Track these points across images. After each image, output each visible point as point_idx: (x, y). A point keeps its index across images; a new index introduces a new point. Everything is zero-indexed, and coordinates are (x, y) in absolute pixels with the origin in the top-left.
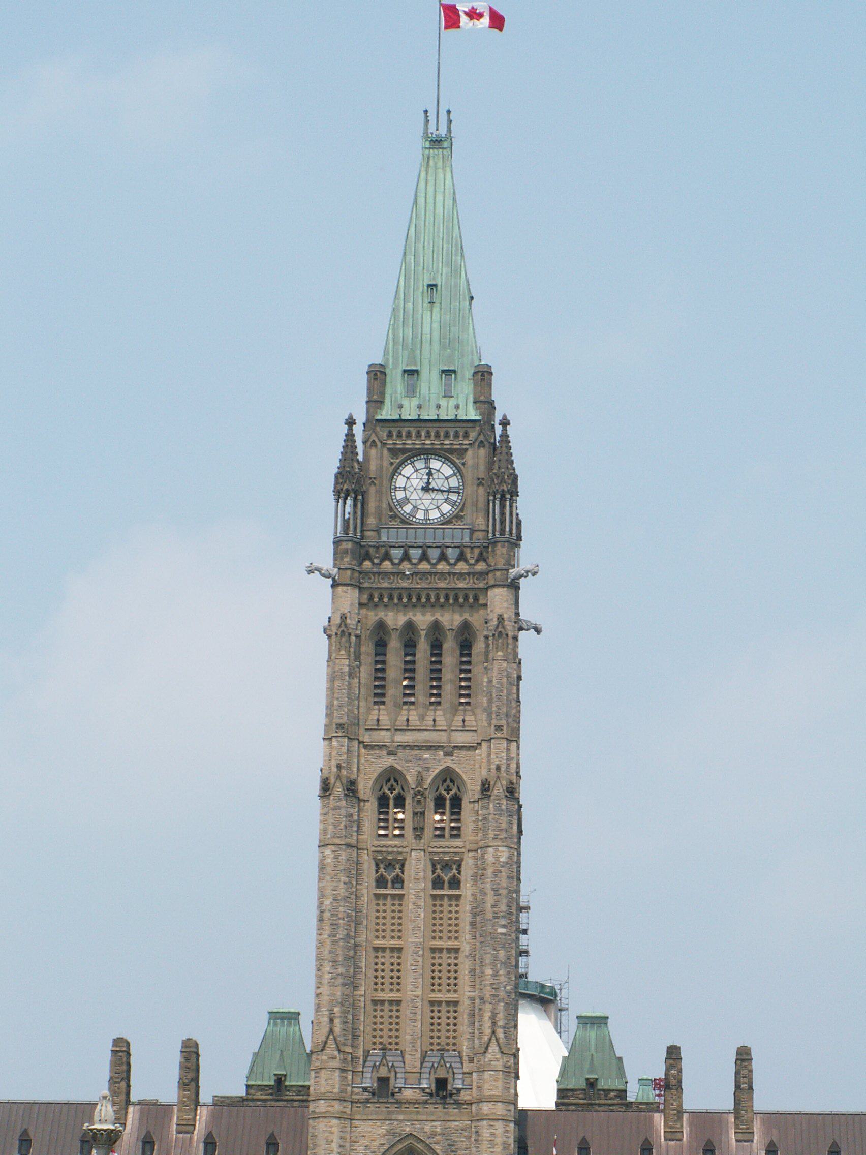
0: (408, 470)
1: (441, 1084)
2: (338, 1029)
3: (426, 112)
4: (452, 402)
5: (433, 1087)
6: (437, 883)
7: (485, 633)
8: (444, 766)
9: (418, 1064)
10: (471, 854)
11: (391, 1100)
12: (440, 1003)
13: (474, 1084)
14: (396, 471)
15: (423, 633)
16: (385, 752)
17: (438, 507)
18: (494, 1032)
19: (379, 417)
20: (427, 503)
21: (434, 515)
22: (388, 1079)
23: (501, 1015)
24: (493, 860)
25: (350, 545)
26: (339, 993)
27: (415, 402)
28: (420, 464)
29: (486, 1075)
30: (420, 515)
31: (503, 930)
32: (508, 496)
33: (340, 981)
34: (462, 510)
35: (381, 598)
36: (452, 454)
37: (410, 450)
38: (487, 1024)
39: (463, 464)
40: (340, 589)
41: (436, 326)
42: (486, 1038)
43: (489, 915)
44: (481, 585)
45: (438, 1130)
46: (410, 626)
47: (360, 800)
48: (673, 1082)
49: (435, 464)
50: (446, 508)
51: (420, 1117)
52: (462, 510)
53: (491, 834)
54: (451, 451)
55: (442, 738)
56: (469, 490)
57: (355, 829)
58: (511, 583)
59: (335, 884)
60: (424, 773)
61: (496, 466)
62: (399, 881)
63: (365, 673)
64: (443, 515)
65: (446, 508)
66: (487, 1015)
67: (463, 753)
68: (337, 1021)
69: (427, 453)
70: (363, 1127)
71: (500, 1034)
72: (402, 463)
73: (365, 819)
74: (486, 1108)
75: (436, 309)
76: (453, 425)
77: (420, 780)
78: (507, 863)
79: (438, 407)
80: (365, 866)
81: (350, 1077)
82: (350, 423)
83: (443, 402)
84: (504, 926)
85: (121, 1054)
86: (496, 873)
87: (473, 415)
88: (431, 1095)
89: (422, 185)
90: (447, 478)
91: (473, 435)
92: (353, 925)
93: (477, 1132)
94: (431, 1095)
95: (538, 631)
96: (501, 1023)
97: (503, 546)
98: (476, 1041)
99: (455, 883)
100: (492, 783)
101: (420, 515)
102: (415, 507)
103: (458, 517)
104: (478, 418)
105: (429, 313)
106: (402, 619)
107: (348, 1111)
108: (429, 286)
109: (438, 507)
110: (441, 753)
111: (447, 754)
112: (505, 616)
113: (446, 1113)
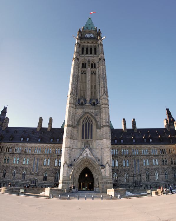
1: (94, 103)
5: (92, 103)
6: (92, 74)
9: (89, 99)
12: (93, 91)
18: (104, 92)
22: (83, 102)
29: (103, 100)
38: (103, 91)
42: (103, 93)
43: (102, 74)
45: (94, 111)
53: (101, 64)
55: (92, 56)
62: (85, 74)
63: (81, 49)
66: (103, 90)
68: (73, 90)
70: (77, 110)
71: (106, 93)
74: (103, 106)
77: (89, 60)
80: (80, 70)
81: (75, 101)
85: (41, 120)
86: (103, 69)
92: (77, 77)
93: (102, 111)
94: (92, 105)
98: (101, 95)
99: (95, 74)
107: (75, 107)
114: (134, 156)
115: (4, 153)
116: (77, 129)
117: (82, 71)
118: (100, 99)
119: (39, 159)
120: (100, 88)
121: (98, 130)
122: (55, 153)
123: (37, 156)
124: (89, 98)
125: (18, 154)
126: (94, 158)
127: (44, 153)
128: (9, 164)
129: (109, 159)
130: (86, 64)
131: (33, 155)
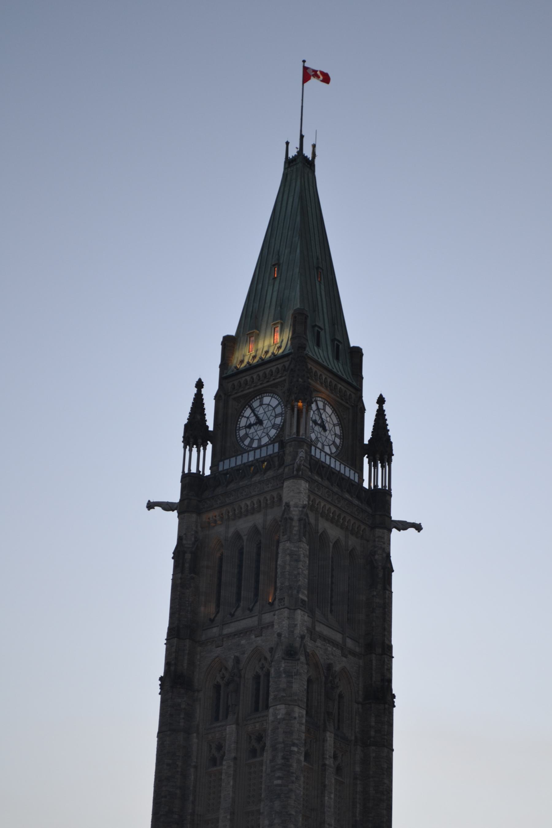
3: (287, 143)
15: (245, 538)
30: (255, 445)
31: (279, 782)
41: (275, 294)
46: (238, 536)
49: (266, 400)
72: (243, 408)
78: (284, 719)
82: (200, 385)
84: (279, 778)
89: (281, 196)
90: (274, 409)
95: (418, 527)
105: (272, 286)
106: (232, 530)
110: (253, 637)
112: (292, 503)
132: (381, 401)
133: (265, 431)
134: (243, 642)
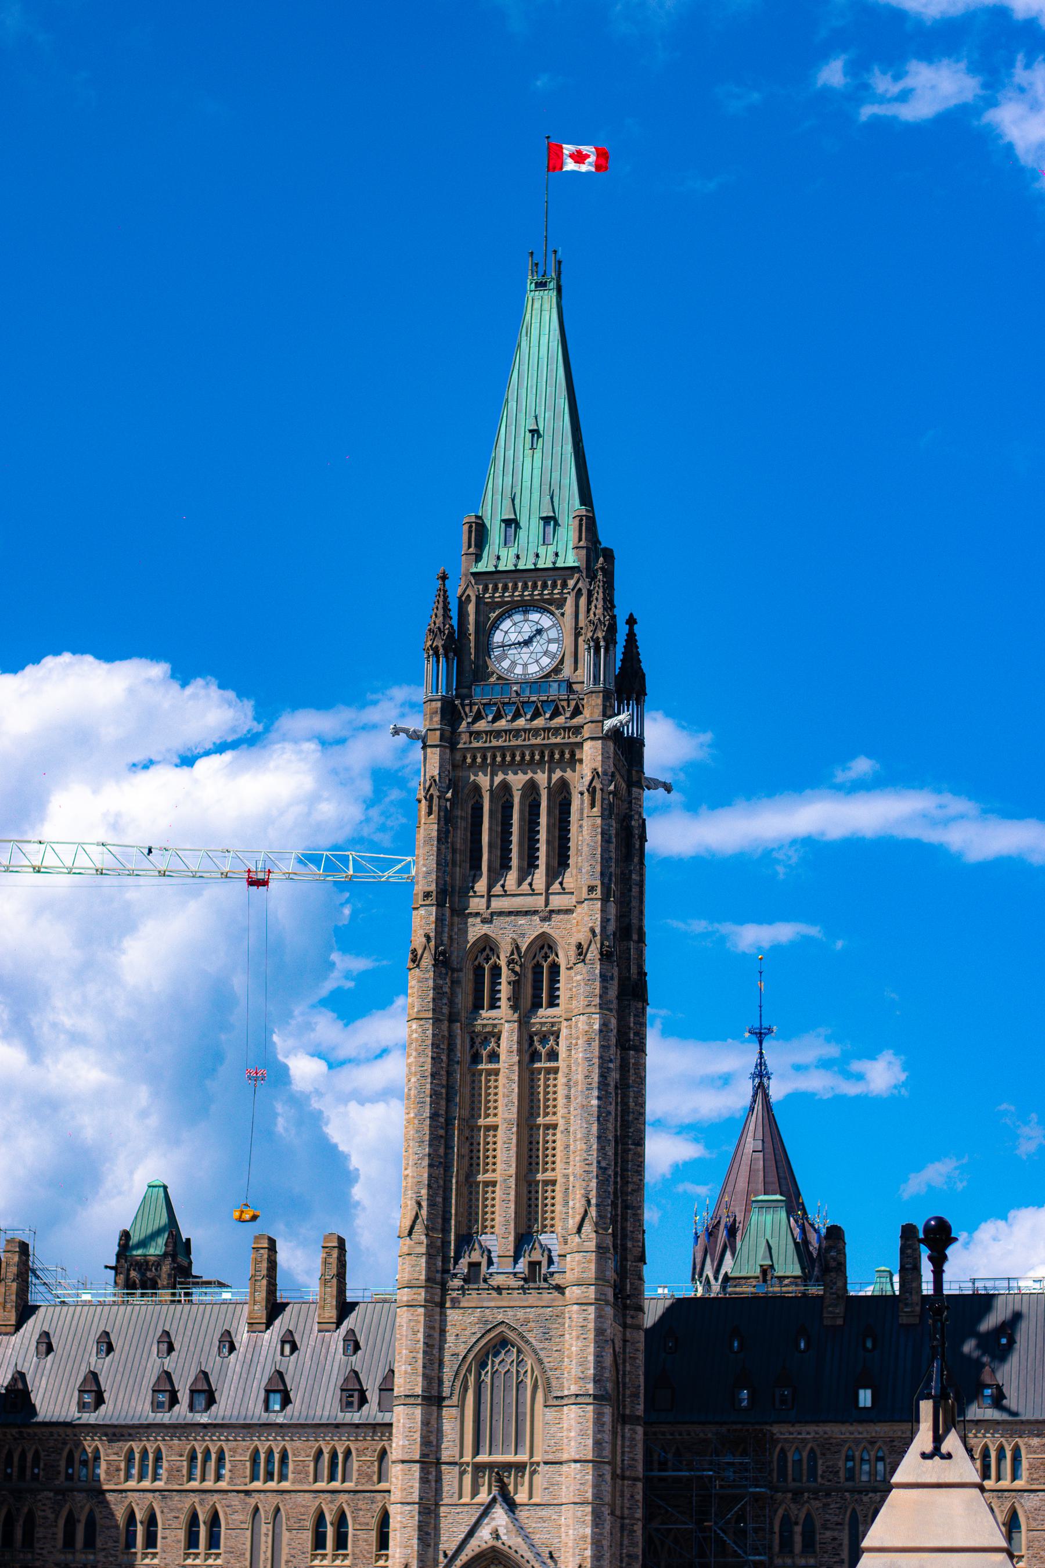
0: (506, 625)
1: (534, 1265)
2: (424, 1212)
4: (551, 549)
7: (580, 789)
8: (541, 931)
9: (511, 1247)
10: (565, 1024)
11: (483, 1285)
13: (568, 1266)
14: (495, 626)
16: (479, 920)
17: (537, 661)
18: (586, 1212)
19: (474, 570)
20: (525, 657)
21: (533, 669)
22: (479, 1264)
23: (593, 1193)
24: (586, 1028)
25: (439, 704)
26: (426, 1175)
27: (513, 551)
28: (518, 617)
30: (519, 670)
32: (602, 643)
33: (426, 1162)
34: (562, 662)
35: (474, 759)
36: (551, 605)
37: (508, 603)
39: (563, 614)
40: (429, 750)
41: (537, 472)
42: (578, 1218)
44: (578, 739)
46: (505, 786)
47: (453, 970)
48: (833, 1264)
50: (545, 661)
51: (512, 1304)
52: (562, 662)
54: (550, 602)
56: (569, 641)
57: (445, 1001)
58: (606, 734)
59: (422, 1060)
60: (519, 941)
61: (592, 613)
63: (460, 837)
64: (542, 669)
65: (545, 661)
67: (561, 916)
69: (525, 607)
72: (500, 618)
73: (459, 990)
75: (538, 454)
76: (551, 573)
79: (537, 556)
80: (459, 1042)
83: (542, 551)
87: (571, 559)
88: (525, 1280)
91: (571, 583)
92: (443, 1103)
96: (593, 1201)
97: (597, 697)
98: (571, 1221)
100: (585, 947)
101: (519, 670)
102: (512, 662)
103: (557, 670)
104: (576, 564)
108: (530, 431)
109: (537, 661)
111: (544, 920)
113: (540, 1299)
114: (852, 1491)
115: (57, 1492)
116: (454, 1412)
117: (472, 1039)
118: (566, 1243)
119: (288, 1519)
120: (571, 1178)
121: (551, 1414)
122: (375, 1478)
123: (274, 1500)
124: (512, 1238)
125: (150, 1495)
126: (525, 1547)
127: (311, 1478)
128: (101, 1557)
129: (588, 1553)
130: (496, 970)
131: (247, 1493)
132: (631, 621)
133: (534, 656)
134: (522, 921)
